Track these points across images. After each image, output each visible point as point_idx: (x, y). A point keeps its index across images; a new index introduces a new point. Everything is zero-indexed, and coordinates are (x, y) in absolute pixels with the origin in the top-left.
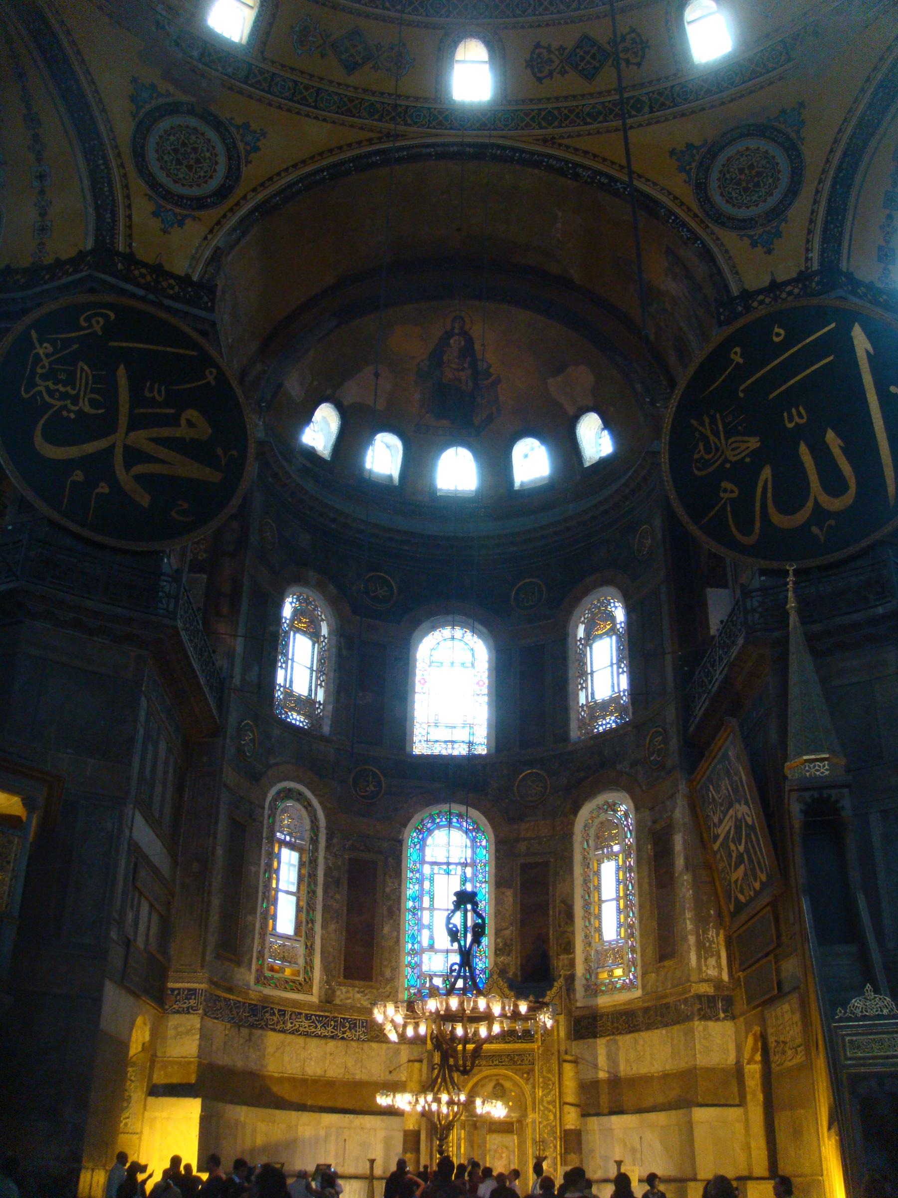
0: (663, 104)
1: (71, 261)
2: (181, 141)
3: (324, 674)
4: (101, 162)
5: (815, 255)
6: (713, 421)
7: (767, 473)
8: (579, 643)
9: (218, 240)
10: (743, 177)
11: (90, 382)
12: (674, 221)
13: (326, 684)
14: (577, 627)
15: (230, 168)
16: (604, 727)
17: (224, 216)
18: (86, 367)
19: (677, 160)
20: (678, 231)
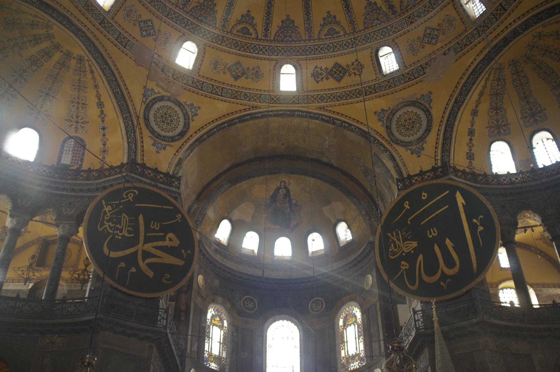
0: (371, 92)
1: (118, 167)
2: (164, 112)
3: (226, 344)
4: (130, 123)
5: (439, 157)
6: (397, 234)
7: (421, 257)
8: (340, 328)
9: (180, 155)
10: (406, 123)
11: (128, 222)
12: (377, 143)
13: (227, 349)
14: (339, 320)
15: (185, 123)
16: (353, 367)
17: (183, 144)
18: (125, 216)
19: (378, 116)
20: (379, 147)
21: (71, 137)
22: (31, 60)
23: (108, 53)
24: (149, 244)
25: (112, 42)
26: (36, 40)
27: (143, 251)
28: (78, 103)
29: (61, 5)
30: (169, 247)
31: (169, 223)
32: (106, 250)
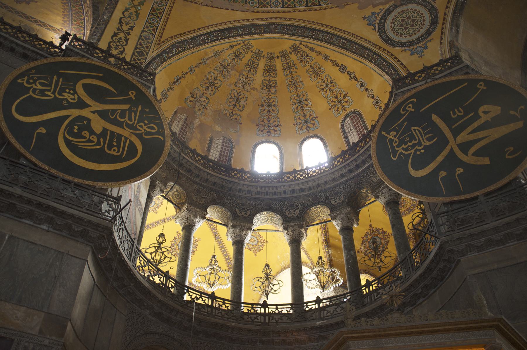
2: (400, 21)
4: (375, 56)
9: (447, 38)
11: (422, 132)
15: (429, 10)
17: (443, 28)
18: (415, 128)
21: (345, 119)
22: (264, 86)
23: (308, 21)
24: (462, 134)
25: (305, 11)
26: (252, 67)
27: (461, 146)
28: (327, 86)
29: (239, 21)
30: (490, 120)
31: (472, 99)
32: (413, 173)
